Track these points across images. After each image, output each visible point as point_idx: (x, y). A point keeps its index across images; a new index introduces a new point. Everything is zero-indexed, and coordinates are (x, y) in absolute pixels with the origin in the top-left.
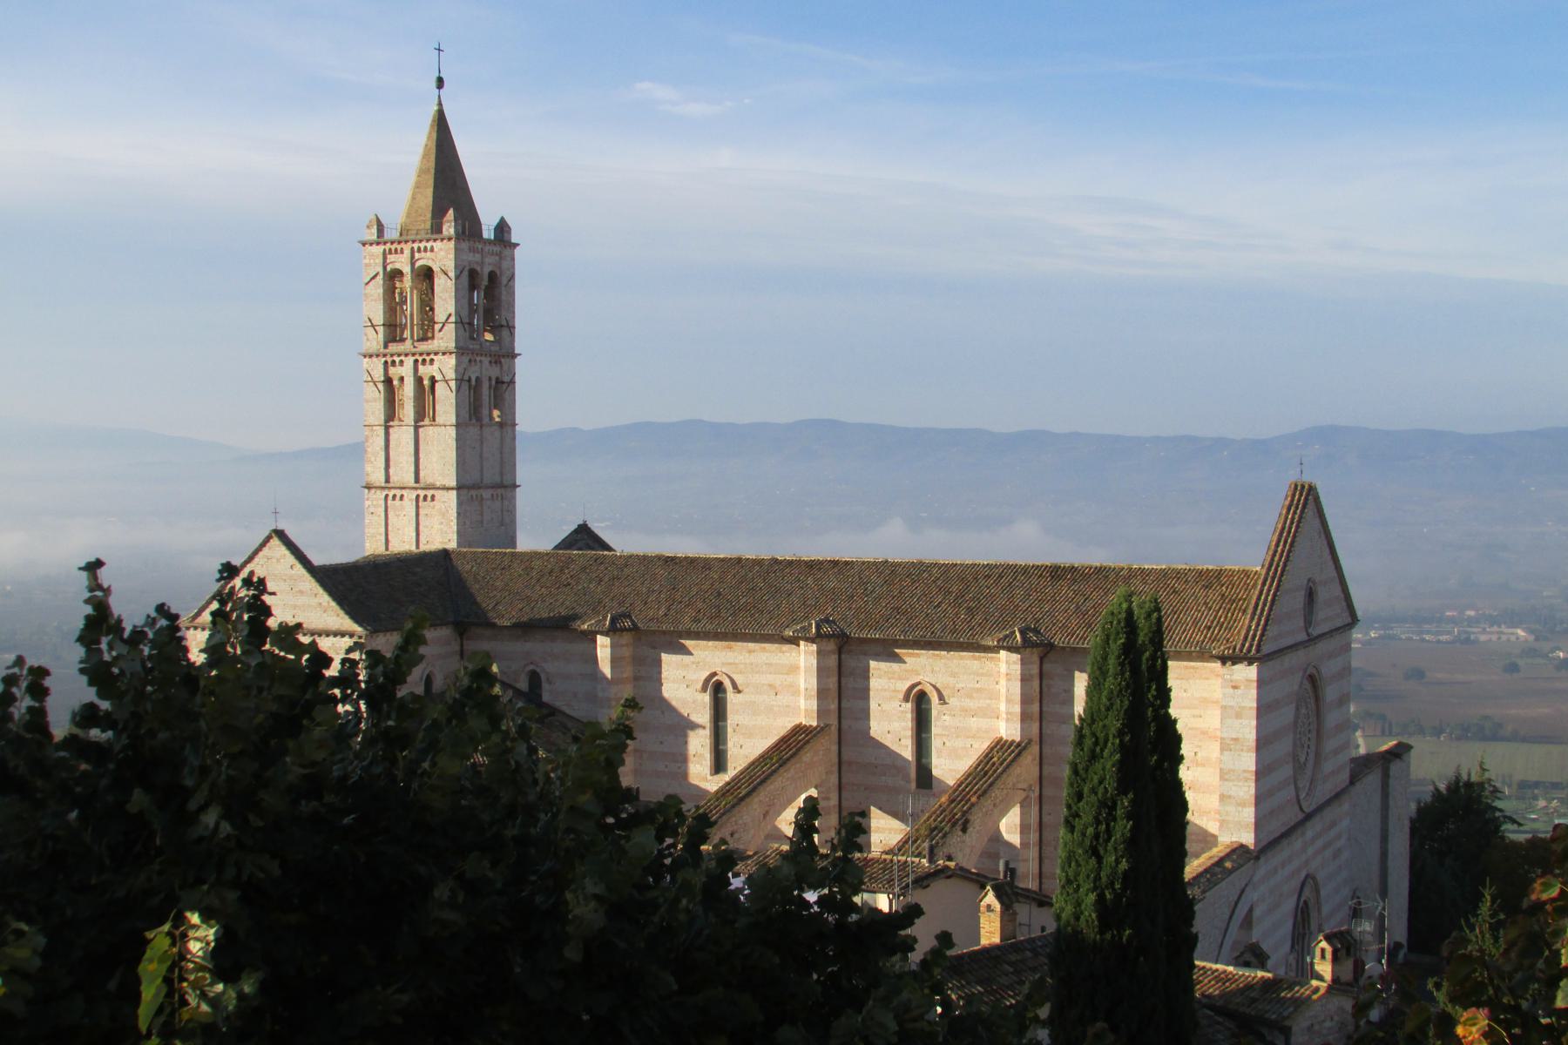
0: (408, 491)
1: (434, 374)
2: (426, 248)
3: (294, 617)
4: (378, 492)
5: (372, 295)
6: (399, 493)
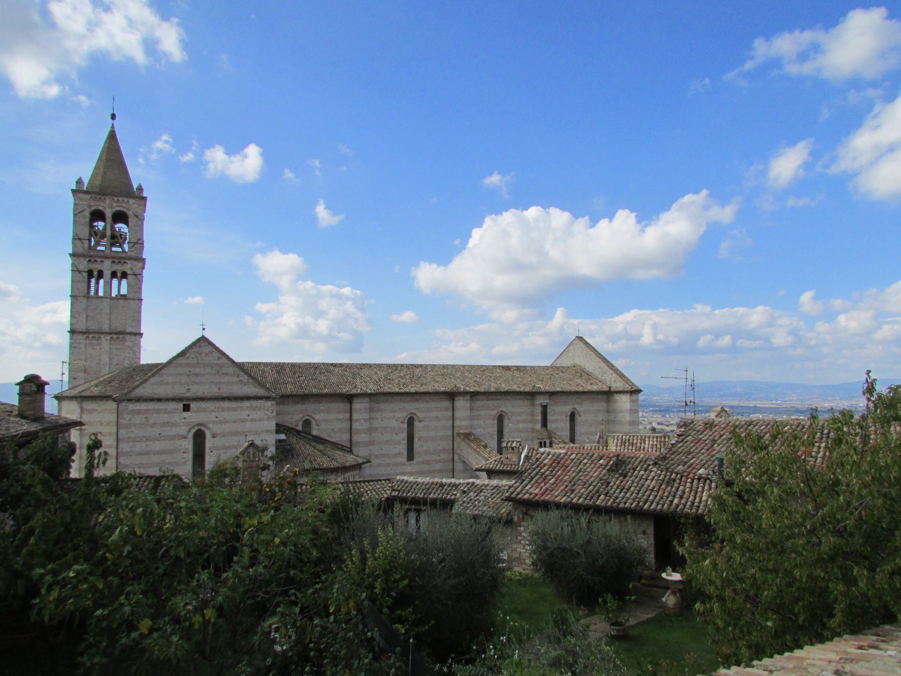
0: (104, 335)
1: (126, 270)
2: (123, 200)
6: (97, 336)
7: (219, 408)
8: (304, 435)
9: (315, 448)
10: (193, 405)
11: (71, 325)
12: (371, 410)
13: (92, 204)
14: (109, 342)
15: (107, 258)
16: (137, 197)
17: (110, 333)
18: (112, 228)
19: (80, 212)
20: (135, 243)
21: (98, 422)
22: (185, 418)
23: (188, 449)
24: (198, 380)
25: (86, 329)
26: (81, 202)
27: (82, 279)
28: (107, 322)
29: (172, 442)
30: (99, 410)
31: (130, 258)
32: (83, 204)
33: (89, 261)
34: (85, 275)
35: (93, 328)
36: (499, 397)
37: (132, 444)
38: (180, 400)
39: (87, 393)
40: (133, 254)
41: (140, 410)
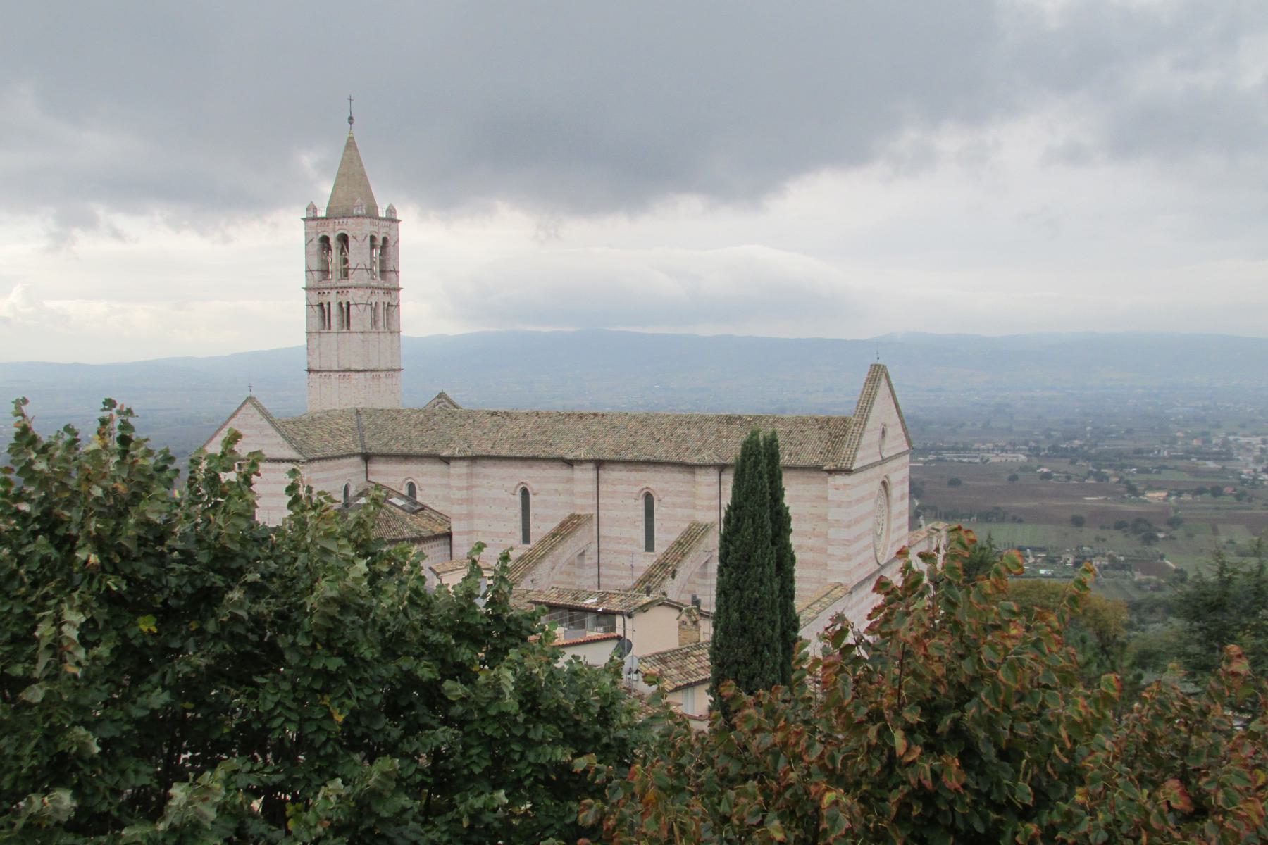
6: (328, 374)
12: (470, 475)
34: (317, 309)
36: (644, 467)
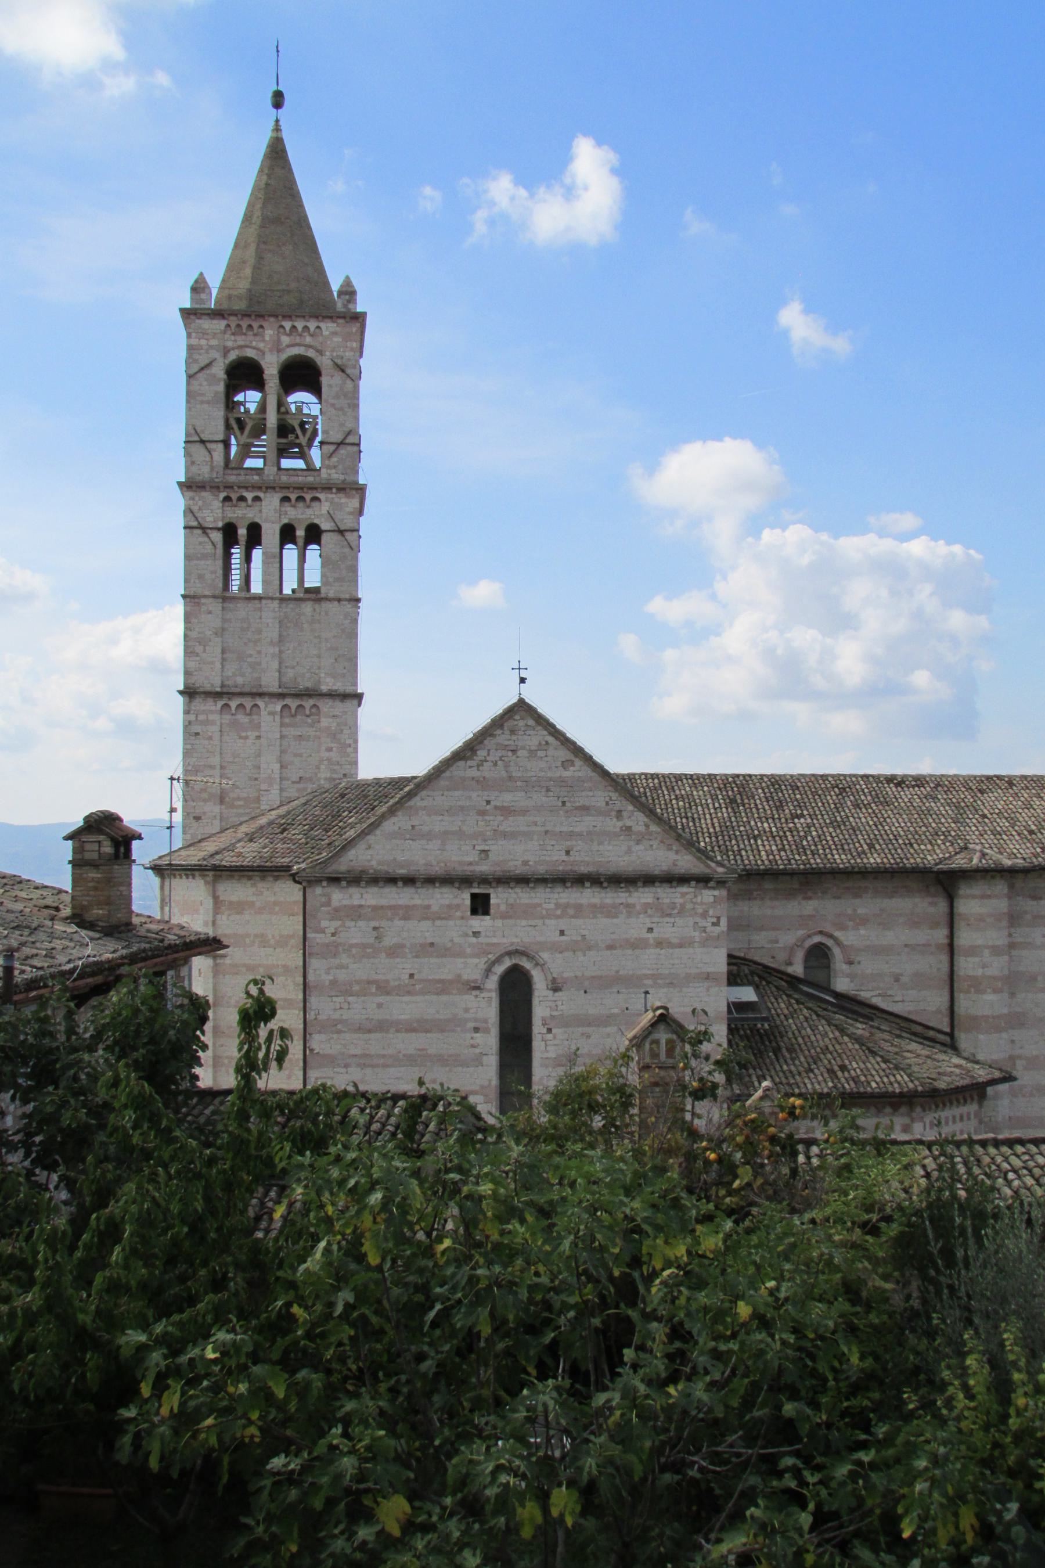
0: (267, 699)
1: (316, 521)
2: (306, 328)
3: (568, 853)
4: (210, 701)
5: (203, 395)
6: (248, 703)
7: (567, 906)
8: (805, 989)
9: (842, 1031)
10: (498, 898)
11: (187, 673)
12: (1014, 919)
13: (230, 344)
14: (278, 718)
15: (270, 488)
16: (342, 316)
17: (282, 696)
18: (281, 404)
19: (202, 369)
20: (340, 444)
21: (256, 936)
22: (476, 934)
23: (486, 1021)
24: (508, 825)
25: (223, 686)
26: (203, 342)
27: (209, 548)
28: (275, 665)
29: (444, 998)
30: (258, 904)
31: (327, 488)
32: (211, 347)
33: (227, 499)
34: (218, 537)
35: (240, 680)
37: (341, 999)
38: (465, 881)
39: (228, 860)
40: (336, 476)
41: (361, 906)
